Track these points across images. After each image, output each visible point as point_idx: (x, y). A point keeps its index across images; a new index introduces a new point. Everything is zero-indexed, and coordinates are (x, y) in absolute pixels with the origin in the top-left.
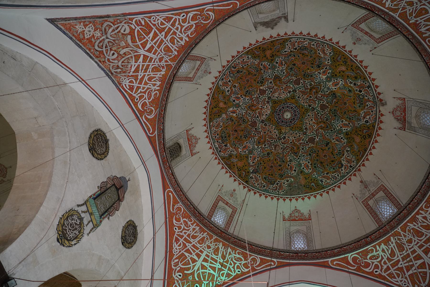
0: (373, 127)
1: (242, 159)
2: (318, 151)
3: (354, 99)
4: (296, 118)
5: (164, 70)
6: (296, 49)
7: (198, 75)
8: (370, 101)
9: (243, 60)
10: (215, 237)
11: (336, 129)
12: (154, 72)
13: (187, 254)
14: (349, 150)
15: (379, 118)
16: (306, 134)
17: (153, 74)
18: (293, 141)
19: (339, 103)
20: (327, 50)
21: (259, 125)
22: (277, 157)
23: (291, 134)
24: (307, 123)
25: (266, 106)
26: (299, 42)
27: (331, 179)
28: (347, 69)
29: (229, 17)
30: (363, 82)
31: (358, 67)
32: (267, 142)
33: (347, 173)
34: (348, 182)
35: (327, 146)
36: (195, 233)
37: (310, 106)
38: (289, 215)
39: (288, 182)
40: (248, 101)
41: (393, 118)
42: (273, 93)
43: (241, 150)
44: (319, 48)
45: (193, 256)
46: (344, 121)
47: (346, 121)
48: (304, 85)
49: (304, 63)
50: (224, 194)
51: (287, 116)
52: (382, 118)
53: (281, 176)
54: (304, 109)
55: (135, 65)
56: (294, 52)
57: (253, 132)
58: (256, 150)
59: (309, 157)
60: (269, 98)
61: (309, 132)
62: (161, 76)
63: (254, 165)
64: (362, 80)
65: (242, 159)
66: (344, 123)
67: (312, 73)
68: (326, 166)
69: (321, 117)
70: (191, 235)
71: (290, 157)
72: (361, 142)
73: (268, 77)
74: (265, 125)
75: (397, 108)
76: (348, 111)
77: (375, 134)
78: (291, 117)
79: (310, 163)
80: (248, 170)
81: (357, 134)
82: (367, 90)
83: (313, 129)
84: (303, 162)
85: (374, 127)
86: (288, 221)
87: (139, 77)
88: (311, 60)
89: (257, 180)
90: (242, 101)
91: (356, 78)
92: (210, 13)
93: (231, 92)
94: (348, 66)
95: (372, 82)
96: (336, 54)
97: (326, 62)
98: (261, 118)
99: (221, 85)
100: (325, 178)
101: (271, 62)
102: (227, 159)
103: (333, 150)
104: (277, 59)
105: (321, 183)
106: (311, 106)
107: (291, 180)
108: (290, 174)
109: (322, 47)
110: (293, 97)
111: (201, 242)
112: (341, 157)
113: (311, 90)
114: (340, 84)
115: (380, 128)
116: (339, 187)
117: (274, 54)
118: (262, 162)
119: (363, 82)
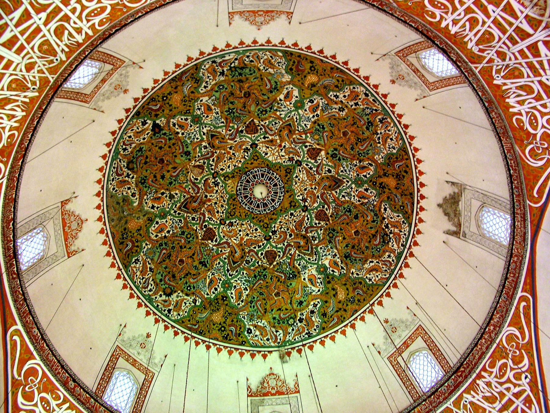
0: (242, 342)
1: (186, 103)
2: (190, 248)
3: (286, 309)
4: (252, 206)
5: (475, 50)
6: (387, 226)
7: (402, 65)
8: (285, 336)
9: (392, 139)
10: (52, 79)
11: (232, 279)
12: (483, 34)
13: (17, 14)
14: (197, 304)
15: (259, 352)
16: (221, 223)
17: (479, 31)
18: (210, 200)
19: (279, 283)
20: (377, 276)
21: (249, 138)
22: (180, 171)
23: (222, 197)
24: (241, 227)
25: (284, 154)
26: (399, 235)
27: (143, 278)
28: (340, 302)
29: (511, 176)
30: (317, 326)
31: (342, 319)
32: (212, 152)
33: (158, 306)
34: (143, 310)
35: (200, 263)
36: (70, 34)
37: (274, 232)
38: (71, 211)
39: (132, 195)
40: (303, 125)
41: (263, 375)
42: (307, 170)
43: (204, 101)
44: (382, 264)
45: (12, 31)
46: (247, 292)
47: (247, 295)
48: (315, 227)
49: (357, 233)
50: (124, 72)
51: (261, 193)
52: (259, 357)
53: (143, 182)
54: (268, 223)
55: (522, 12)
56: (382, 223)
57: (236, 127)
58: (200, 129)
59: (178, 232)
60: (299, 163)
61: (225, 229)
62: (466, 40)
63: (169, 126)
64: (321, 324)
65: (186, 103)
66: (244, 292)
67: (335, 243)
68: (164, 266)
69: (253, 251)
70: (66, 25)
71: (179, 195)
72: (214, 325)
73: (342, 169)
74: (246, 150)
75: (280, 380)
76: (265, 299)
77: (231, 348)
78: (255, 198)
79: (167, 235)
80: (161, 115)
81: (226, 315)
82: (304, 331)
83: (230, 237)
84: (168, 221)
85: (242, 344)
86: (62, 213)
87: (490, 8)
88: (360, 247)
89: (139, 134)
90: (306, 114)
91: (324, 315)
92: (541, 163)
93: (331, 100)
94: (345, 304)
95: (318, 341)
96: (368, 289)
97: (354, 271)
98: (262, 142)
99: (356, 89)
100: (143, 266)
101: (371, 181)
102: (193, 74)
103: (194, 275)
104: (374, 191)
105: (134, 260)
106: (273, 235)
107: (135, 202)
108: (145, 197)
109: (384, 269)
110: (293, 205)
111: (45, 47)
112: (182, 291)
113: (304, 237)
114: (313, 288)
115: (242, 354)
116: (132, 296)
117: (387, 190)
118: (173, 141)
119: (317, 326)
